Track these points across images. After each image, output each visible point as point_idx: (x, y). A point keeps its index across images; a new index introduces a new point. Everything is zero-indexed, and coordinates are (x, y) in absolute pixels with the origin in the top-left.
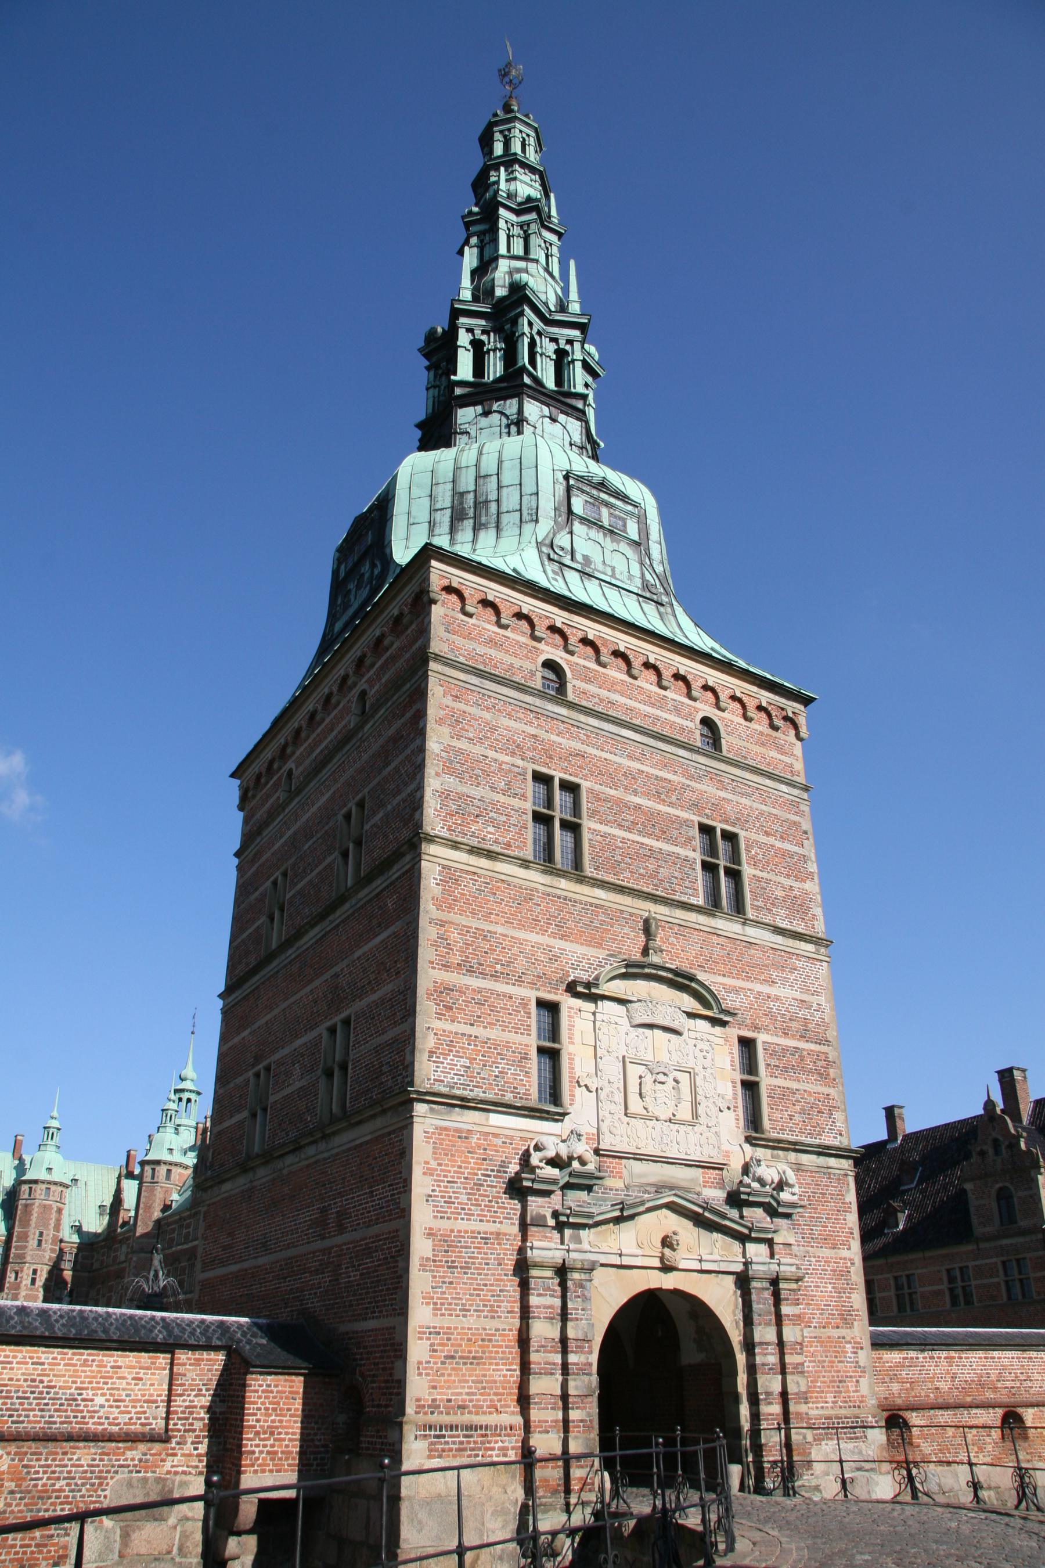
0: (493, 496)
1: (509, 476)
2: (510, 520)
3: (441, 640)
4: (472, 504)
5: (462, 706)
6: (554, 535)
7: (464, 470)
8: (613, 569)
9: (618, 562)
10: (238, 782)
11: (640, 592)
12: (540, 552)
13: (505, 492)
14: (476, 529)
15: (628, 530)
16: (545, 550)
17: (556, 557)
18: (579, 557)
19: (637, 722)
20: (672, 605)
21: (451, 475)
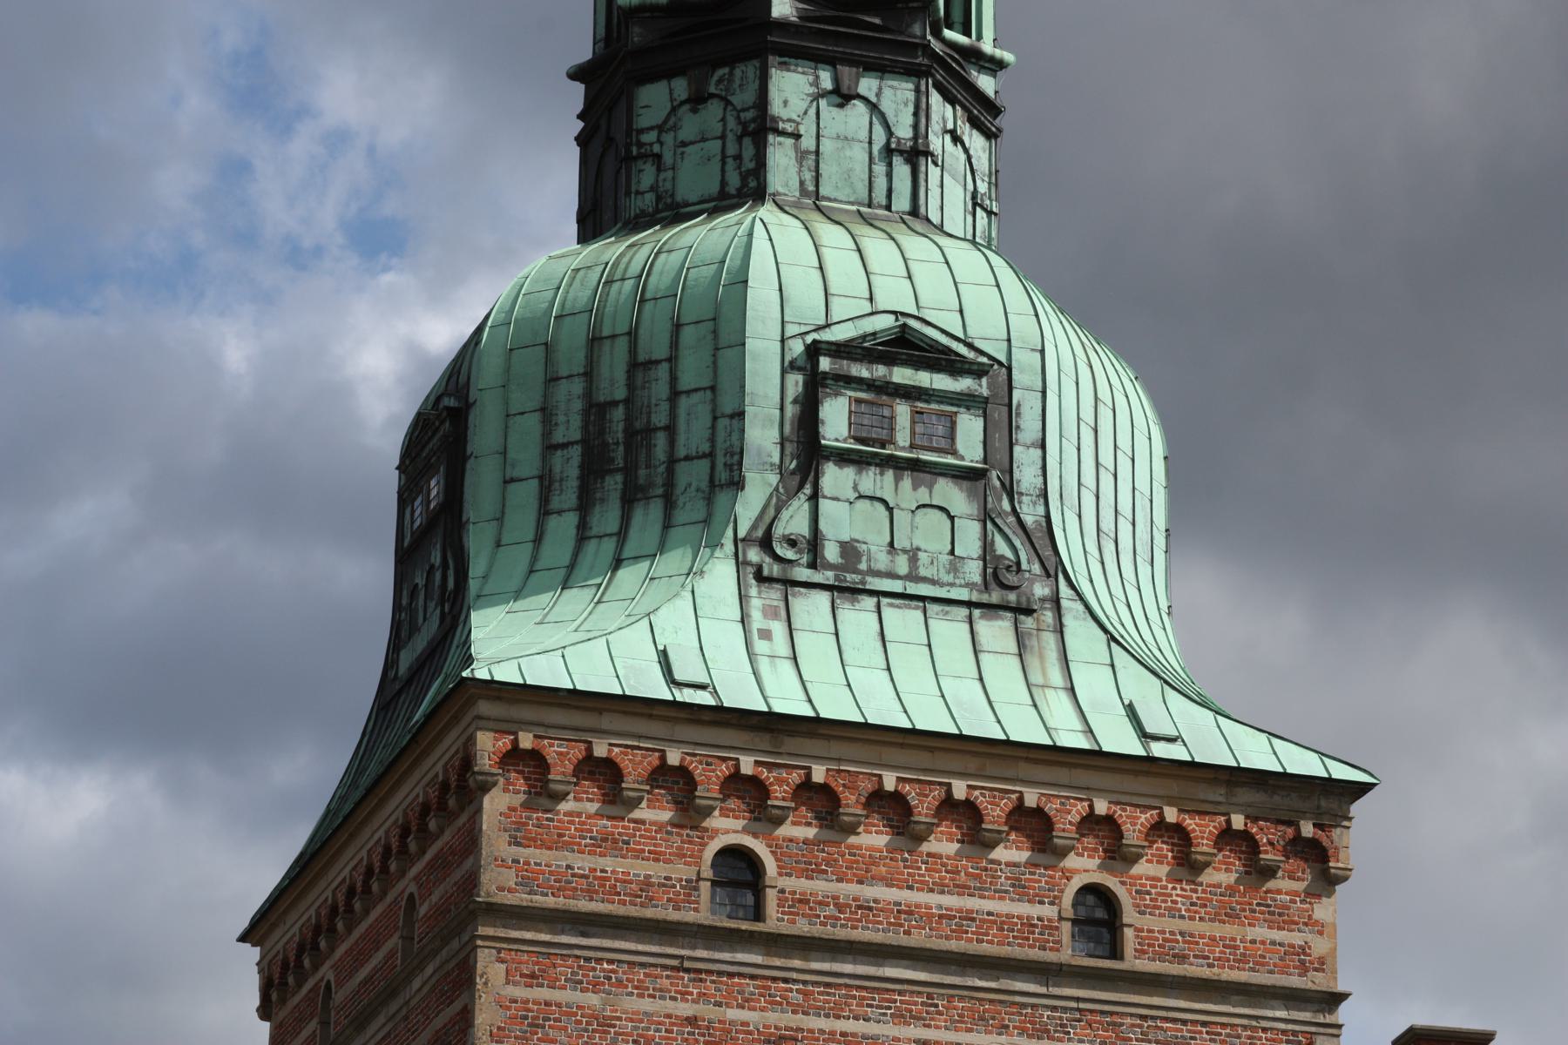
0: (660, 418)
1: (692, 372)
2: (692, 475)
3: (503, 863)
4: (620, 435)
5: (544, 993)
6: (778, 511)
7: (607, 344)
8: (913, 554)
9: (929, 535)
10: (253, 953)
11: (975, 597)
12: (740, 563)
13: (684, 402)
14: (631, 498)
15: (960, 446)
16: (754, 555)
17: (775, 570)
18: (831, 553)
19: (919, 938)
20: (1056, 601)
21: (581, 356)
